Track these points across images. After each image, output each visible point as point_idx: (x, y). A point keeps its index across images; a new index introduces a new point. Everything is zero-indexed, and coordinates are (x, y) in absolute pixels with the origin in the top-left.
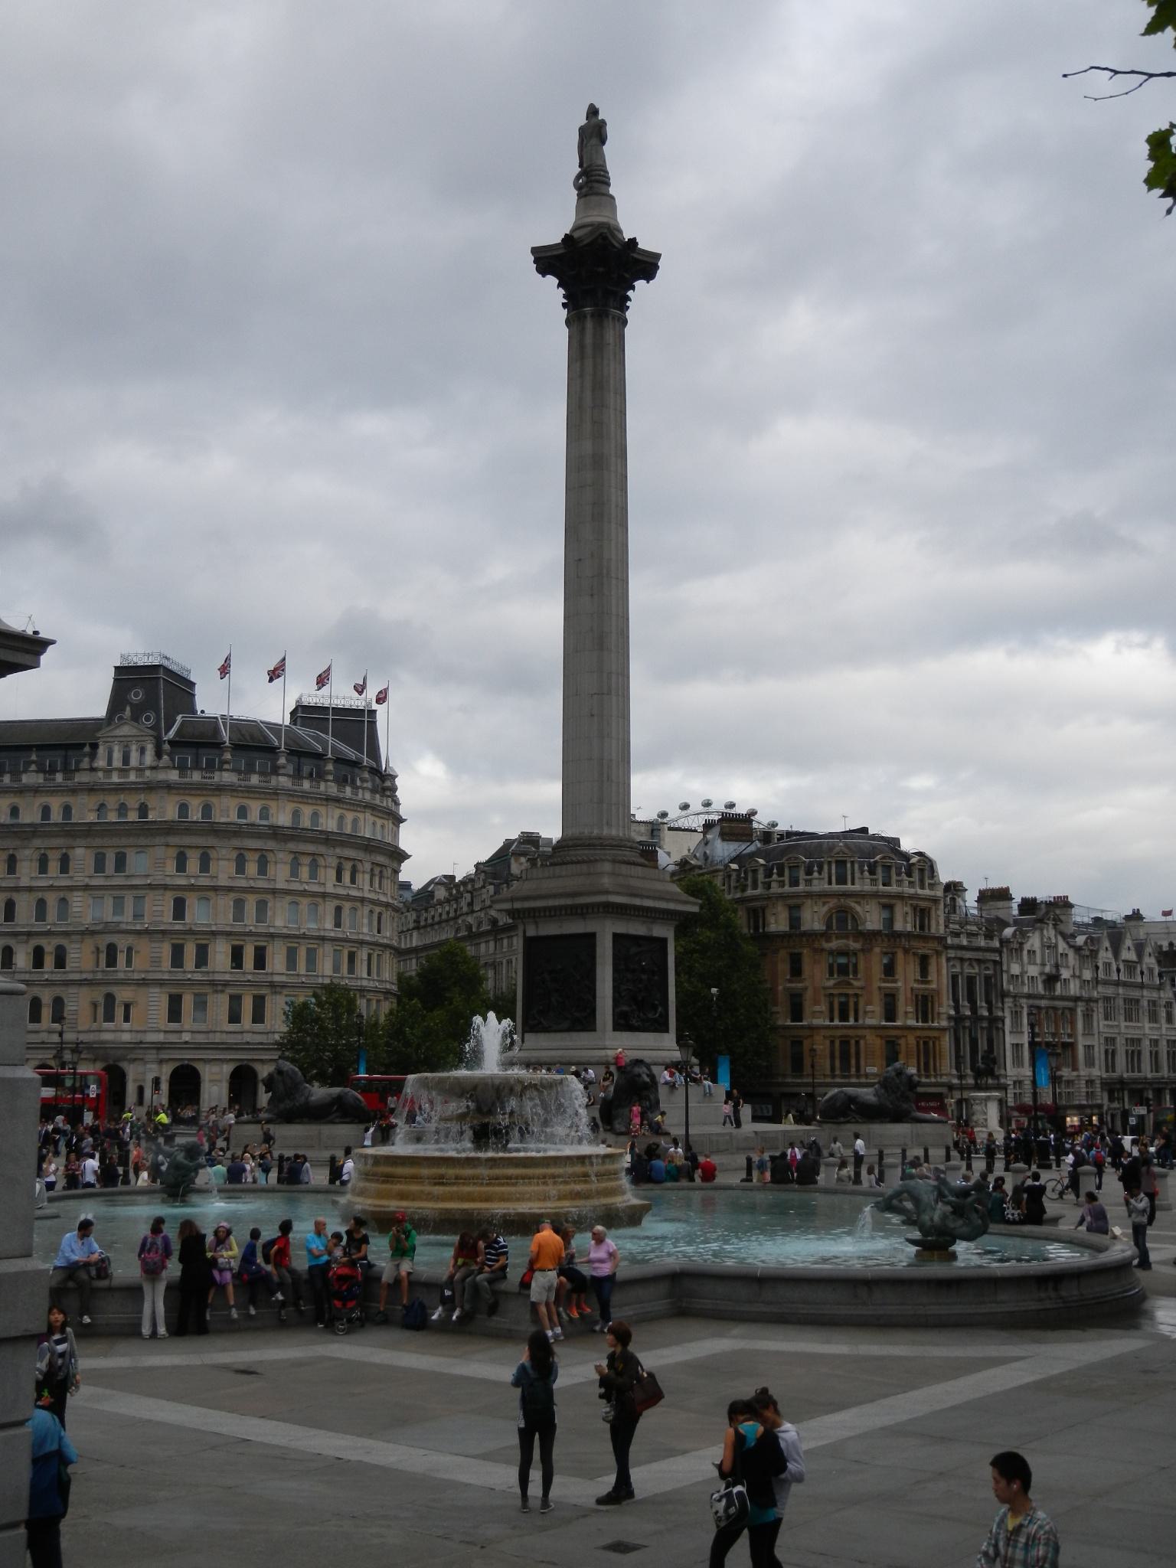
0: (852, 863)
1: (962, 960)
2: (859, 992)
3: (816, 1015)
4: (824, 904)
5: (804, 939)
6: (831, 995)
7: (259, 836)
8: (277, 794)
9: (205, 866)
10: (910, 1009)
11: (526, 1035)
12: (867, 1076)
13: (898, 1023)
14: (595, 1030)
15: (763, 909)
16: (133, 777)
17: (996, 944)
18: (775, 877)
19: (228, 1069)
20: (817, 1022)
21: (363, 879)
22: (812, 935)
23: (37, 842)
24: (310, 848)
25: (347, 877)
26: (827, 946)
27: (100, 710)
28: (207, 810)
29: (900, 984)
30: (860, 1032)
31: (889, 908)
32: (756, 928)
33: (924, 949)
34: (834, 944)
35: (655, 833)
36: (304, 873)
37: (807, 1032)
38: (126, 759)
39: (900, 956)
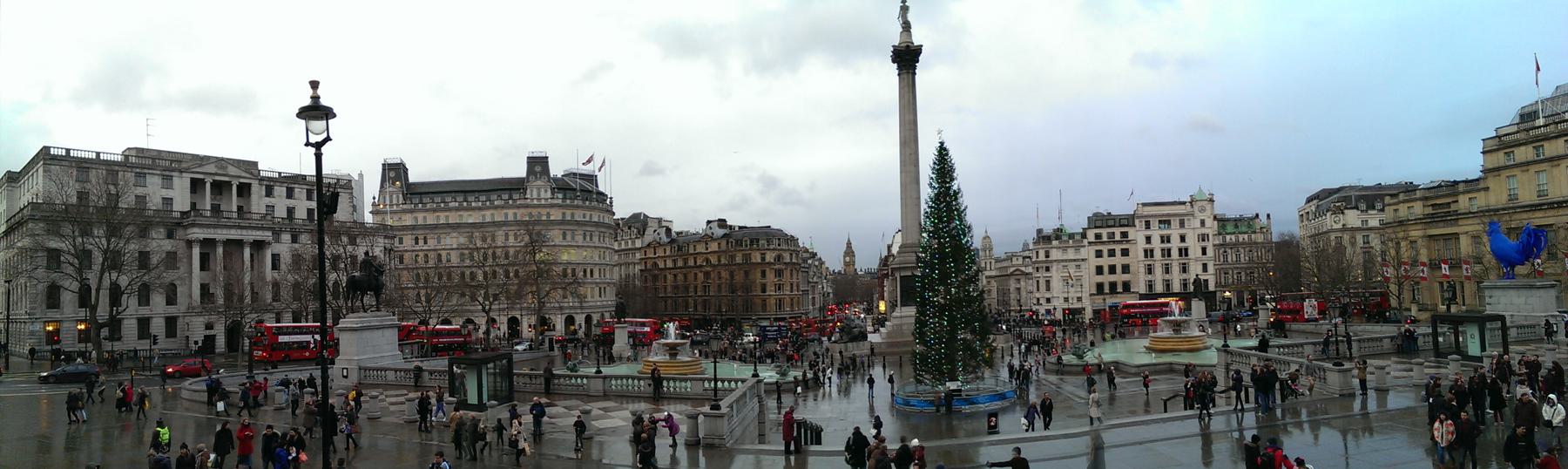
1: (802, 272)
3: (770, 291)
7: (591, 226)
9: (573, 238)
15: (750, 254)
16: (543, 202)
19: (584, 316)
21: (596, 239)
22: (769, 263)
23: (504, 228)
24: (603, 230)
25: (588, 238)
26: (775, 267)
27: (524, 174)
28: (573, 215)
32: (747, 261)
34: (777, 267)
36: (569, 237)
38: (539, 195)
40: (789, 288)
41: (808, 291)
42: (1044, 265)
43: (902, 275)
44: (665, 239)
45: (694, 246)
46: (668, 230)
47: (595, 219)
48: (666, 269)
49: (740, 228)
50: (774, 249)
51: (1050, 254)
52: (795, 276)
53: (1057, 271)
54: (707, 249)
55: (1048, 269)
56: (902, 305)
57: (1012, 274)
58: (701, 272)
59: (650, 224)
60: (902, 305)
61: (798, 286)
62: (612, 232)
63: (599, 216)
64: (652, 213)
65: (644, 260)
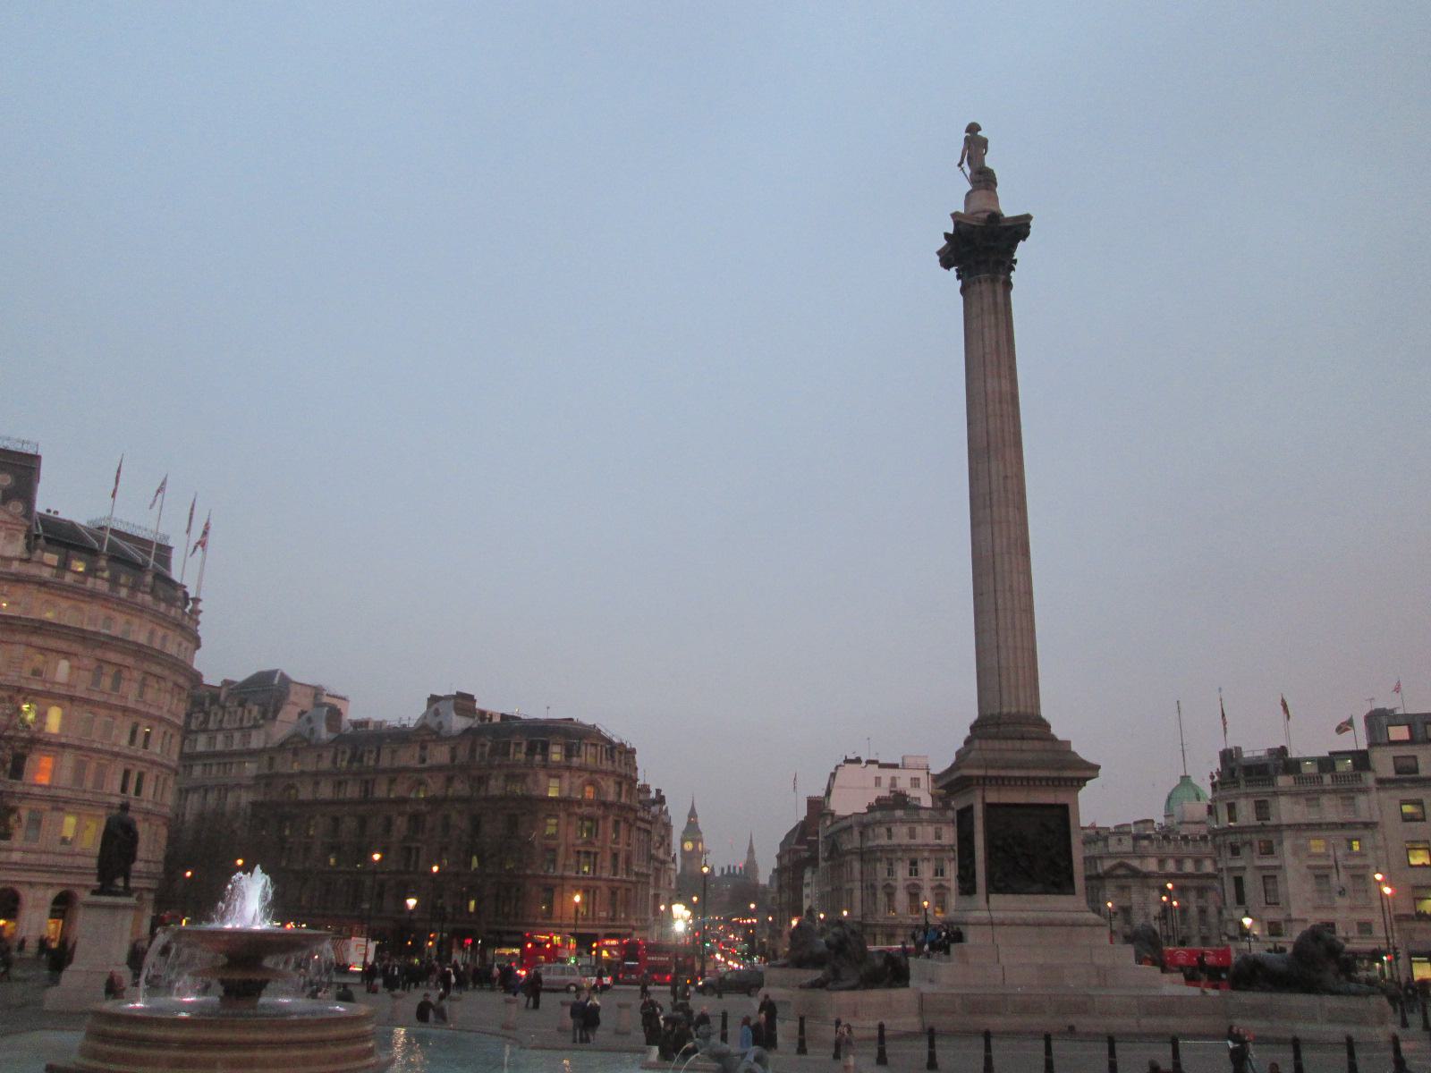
0: (601, 746)
1: (639, 829)
2: (597, 850)
4: (580, 777)
5: (561, 805)
6: (579, 852)
8: (141, 611)
10: (624, 867)
11: (992, 897)
12: (599, 919)
13: (618, 877)
14: (1074, 894)
17: (650, 818)
18: (539, 750)
19: (51, 894)
20: (567, 873)
26: (577, 810)
29: (620, 846)
30: (599, 883)
31: (620, 784)
33: (631, 816)
34: (585, 810)
35: (319, 696)
37: (558, 881)
39: (622, 824)
40: (608, 863)
41: (648, 876)
42: (1255, 838)
43: (993, 797)
44: (324, 734)
45: (394, 752)
46: (335, 715)
47: (142, 638)
48: (317, 803)
49: (504, 717)
50: (579, 769)
51: (1272, 810)
52: (623, 833)
53: (1295, 853)
54: (423, 760)
55: (1268, 850)
56: (995, 887)
57: (1108, 875)
58: (401, 814)
59: (292, 698)
60: (988, 893)
61: (628, 861)
62: (181, 680)
63: (152, 633)
64: (299, 672)
65: (265, 780)
